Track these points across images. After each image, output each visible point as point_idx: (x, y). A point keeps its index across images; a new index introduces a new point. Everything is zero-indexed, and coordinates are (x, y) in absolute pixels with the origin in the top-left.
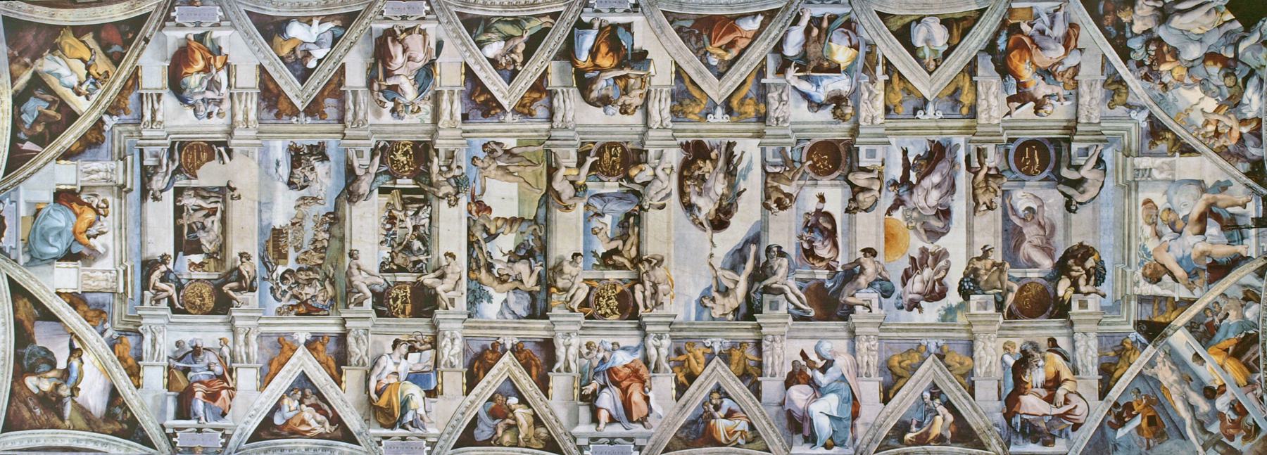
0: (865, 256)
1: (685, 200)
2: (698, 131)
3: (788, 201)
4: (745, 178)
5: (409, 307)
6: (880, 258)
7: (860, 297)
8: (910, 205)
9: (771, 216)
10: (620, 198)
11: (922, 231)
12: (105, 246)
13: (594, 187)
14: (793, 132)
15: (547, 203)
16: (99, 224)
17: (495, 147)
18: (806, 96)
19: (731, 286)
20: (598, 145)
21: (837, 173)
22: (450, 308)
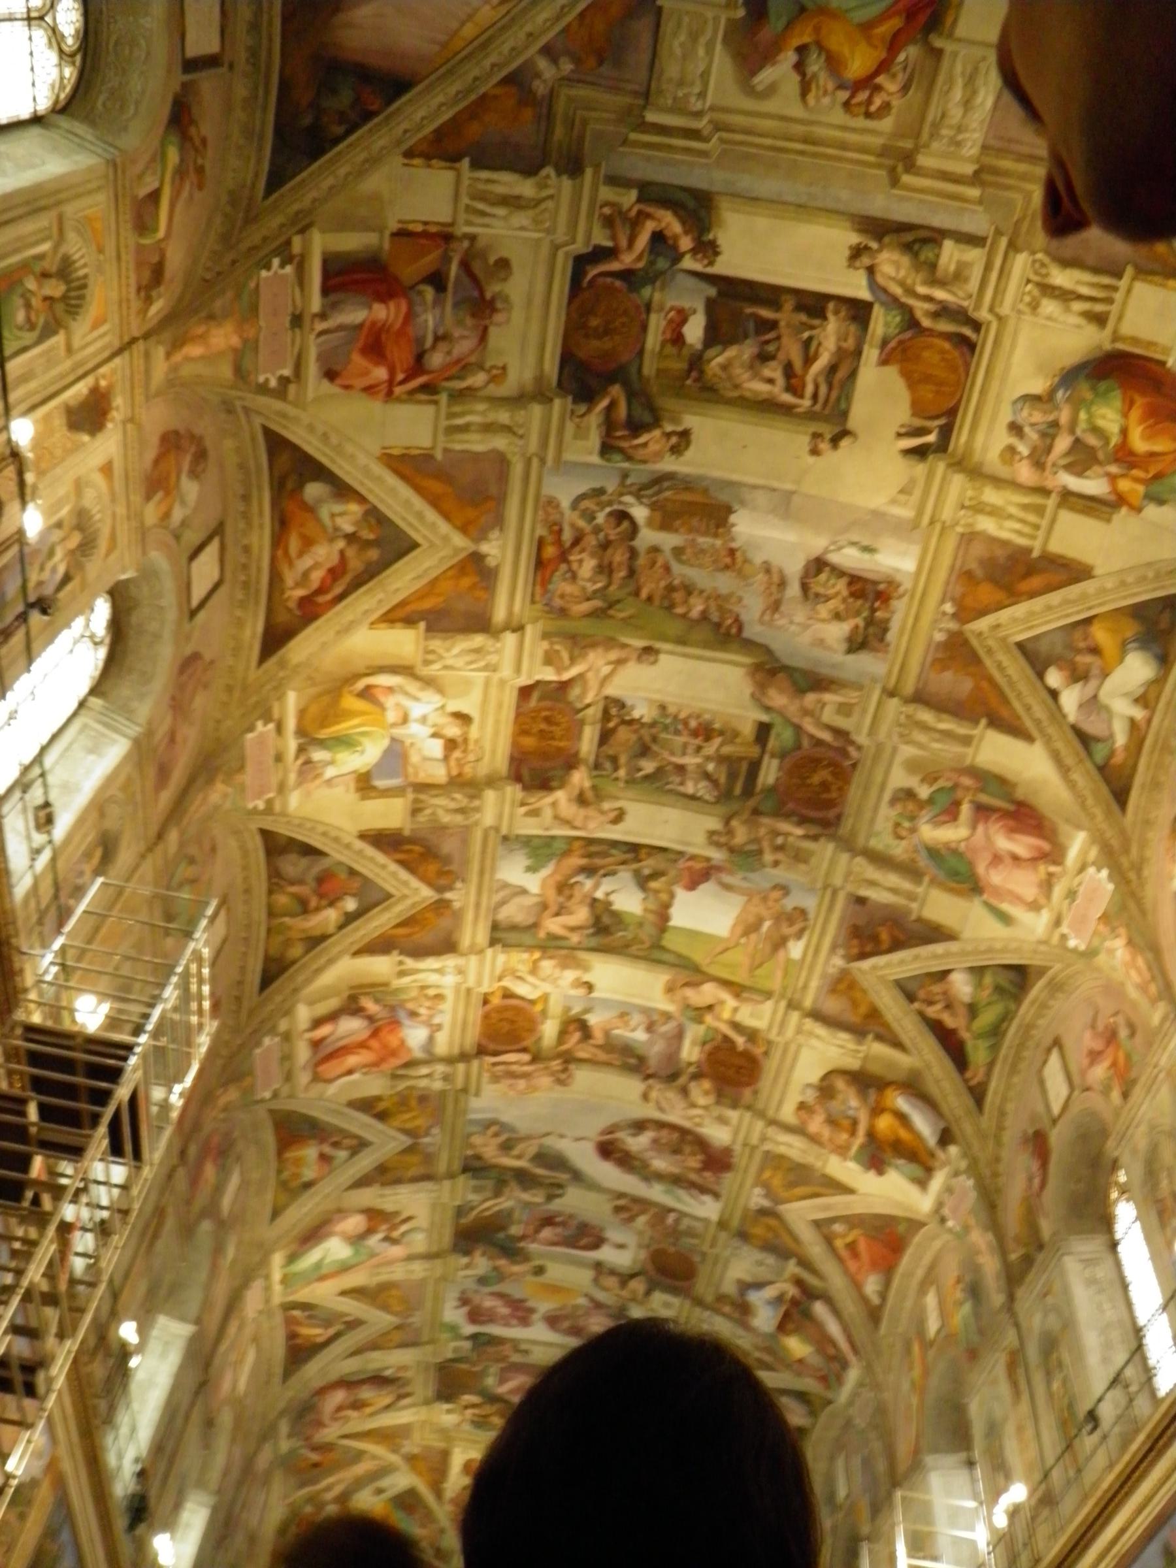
2: (746, 1170)
4: (667, 1192)
5: (529, 742)
6: (530, 1278)
10: (672, 1056)
12: (771, 90)
13: (694, 1032)
15: (685, 967)
16: (830, 86)
17: (797, 927)
18: (759, 1285)
19: (515, 1152)
20: (760, 1057)
22: (523, 810)
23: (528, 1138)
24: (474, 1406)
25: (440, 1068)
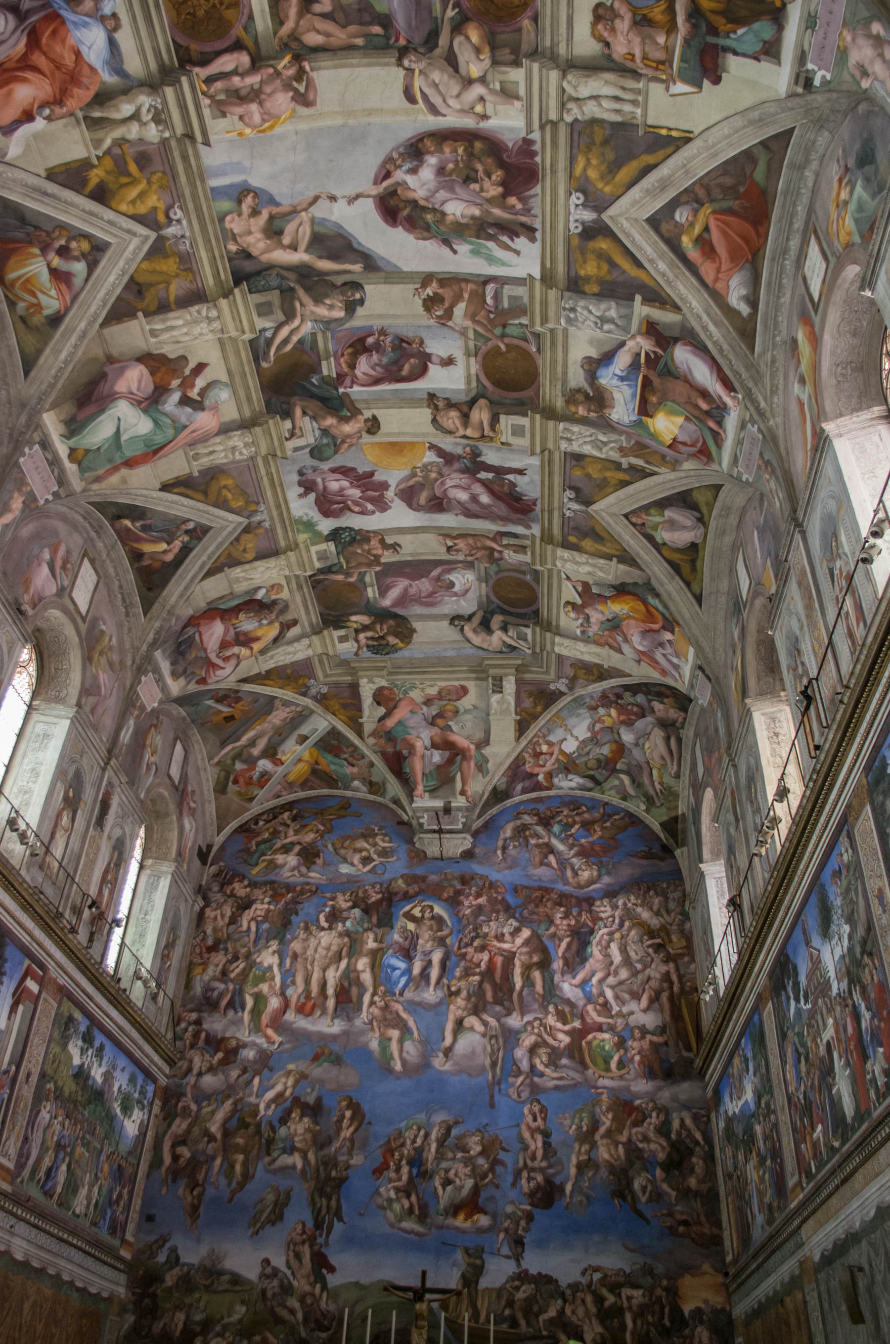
0: (366, 421)
1: (428, 143)
2: (554, 172)
3: (438, 313)
4: (476, 252)
6: (366, 438)
7: (306, 423)
8: (445, 470)
9: (412, 287)
11: (411, 483)
14: (552, 331)
18: (607, 358)
19: (286, 240)
21: (487, 383)
23: (294, 212)
24: (365, 628)
25: (145, 100)
